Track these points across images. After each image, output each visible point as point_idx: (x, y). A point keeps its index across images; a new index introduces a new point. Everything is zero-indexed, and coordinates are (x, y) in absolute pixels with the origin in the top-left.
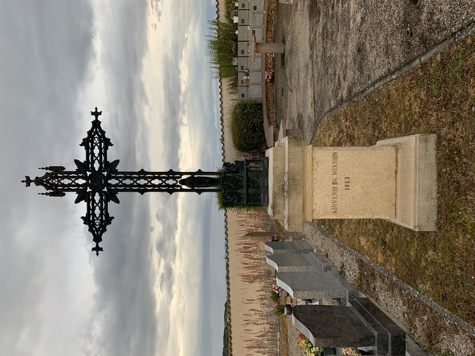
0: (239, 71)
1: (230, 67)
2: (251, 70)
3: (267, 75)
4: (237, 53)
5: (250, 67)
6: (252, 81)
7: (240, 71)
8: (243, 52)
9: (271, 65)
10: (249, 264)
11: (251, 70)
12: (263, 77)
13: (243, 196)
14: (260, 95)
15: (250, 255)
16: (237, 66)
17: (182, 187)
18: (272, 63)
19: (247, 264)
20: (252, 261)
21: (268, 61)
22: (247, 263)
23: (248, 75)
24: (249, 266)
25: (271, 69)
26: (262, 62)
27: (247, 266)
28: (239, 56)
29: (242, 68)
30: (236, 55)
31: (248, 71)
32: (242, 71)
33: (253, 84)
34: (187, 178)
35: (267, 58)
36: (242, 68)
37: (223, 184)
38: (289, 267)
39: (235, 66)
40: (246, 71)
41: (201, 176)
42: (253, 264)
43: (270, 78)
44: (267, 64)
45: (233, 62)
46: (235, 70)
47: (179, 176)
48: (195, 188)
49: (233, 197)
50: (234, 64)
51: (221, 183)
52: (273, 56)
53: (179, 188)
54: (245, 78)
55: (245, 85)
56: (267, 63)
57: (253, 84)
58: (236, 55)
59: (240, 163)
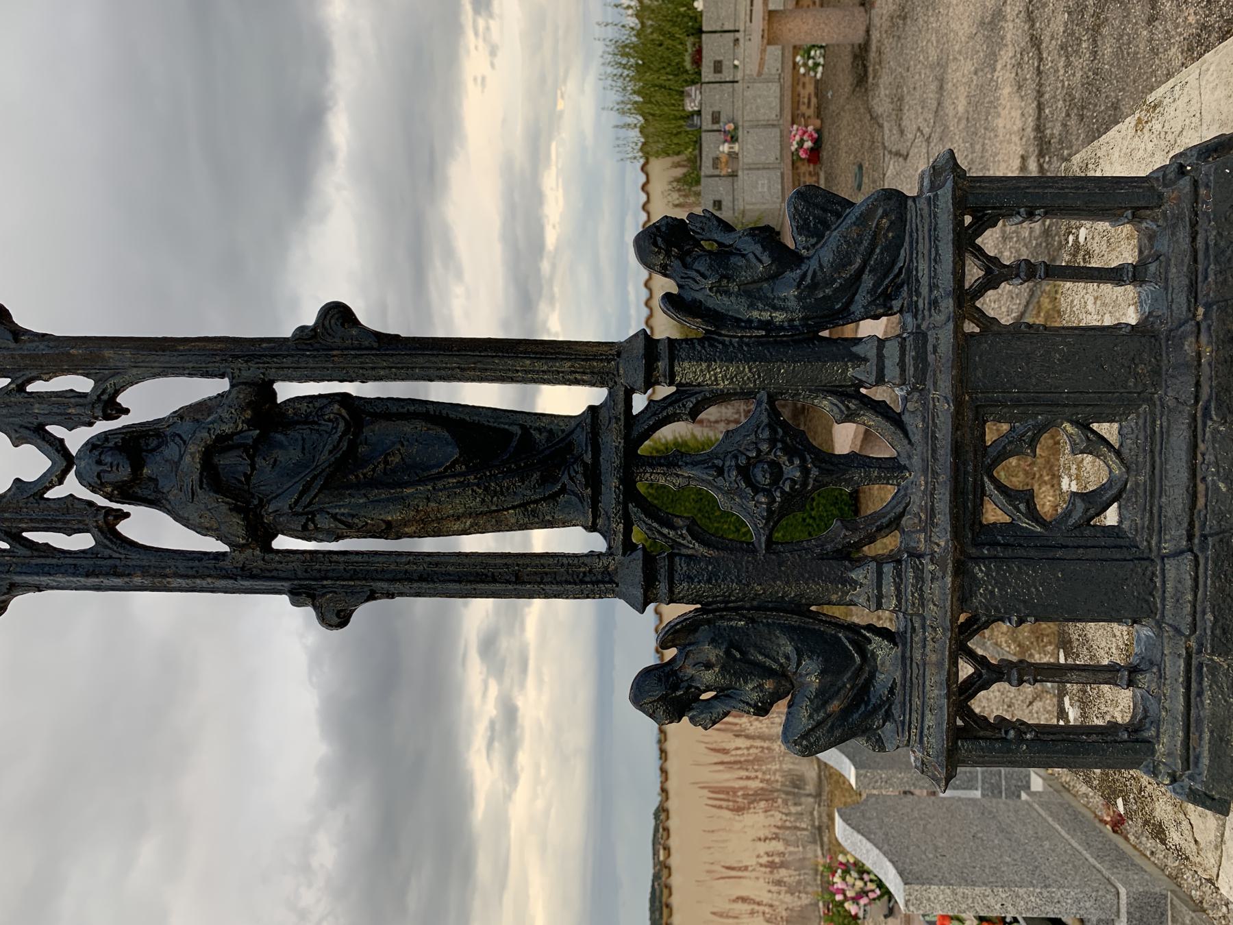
0: (704, 128)
1: (676, 118)
2: (746, 124)
3: (798, 138)
4: (699, 74)
5: (740, 112)
6: (747, 158)
7: (711, 127)
8: (718, 66)
9: (809, 106)
10: (734, 753)
11: (746, 124)
12: (784, 144)
13: (905, 661)
14: (775, 203)
15: (736, 724)
16: (699, 113)
17: (123, 528)
18: (814, 100)
19: (725, 751)
20: (741, 742)
21: (799, 95)
22: (724, 749)
23: (733, 139)
24: (732, 759)
25: (809, 117)
26: (782, 96)
27: (726, 758)
28: (707, 80)
29: (716, 118)
30: (696, 79)
31: (736, 128)
32: (716, 127)
33: (750, 169)
34: (180, 414)
35: (798, 84)
36: (716, 118)
37: (629, 492)
38: (960, 890)
39: (692, 114)
40: (730, 127)
41: (352, 388)
42: (745, 752)
43: (808, 144)
44: (796, 104)
45: (687, 101)
46: (692, 126)
47: (83, 384)
48: (283, 542)
49: (769, 673)
50: (690, 106)
51: (611, 484)
52: (819, 76)
53: (83, 541)
54: (725, 148)
55: (724, 173)
56: (799, 102)
57: (752, 166)
58: (696, 79)
59: (863, 219)
